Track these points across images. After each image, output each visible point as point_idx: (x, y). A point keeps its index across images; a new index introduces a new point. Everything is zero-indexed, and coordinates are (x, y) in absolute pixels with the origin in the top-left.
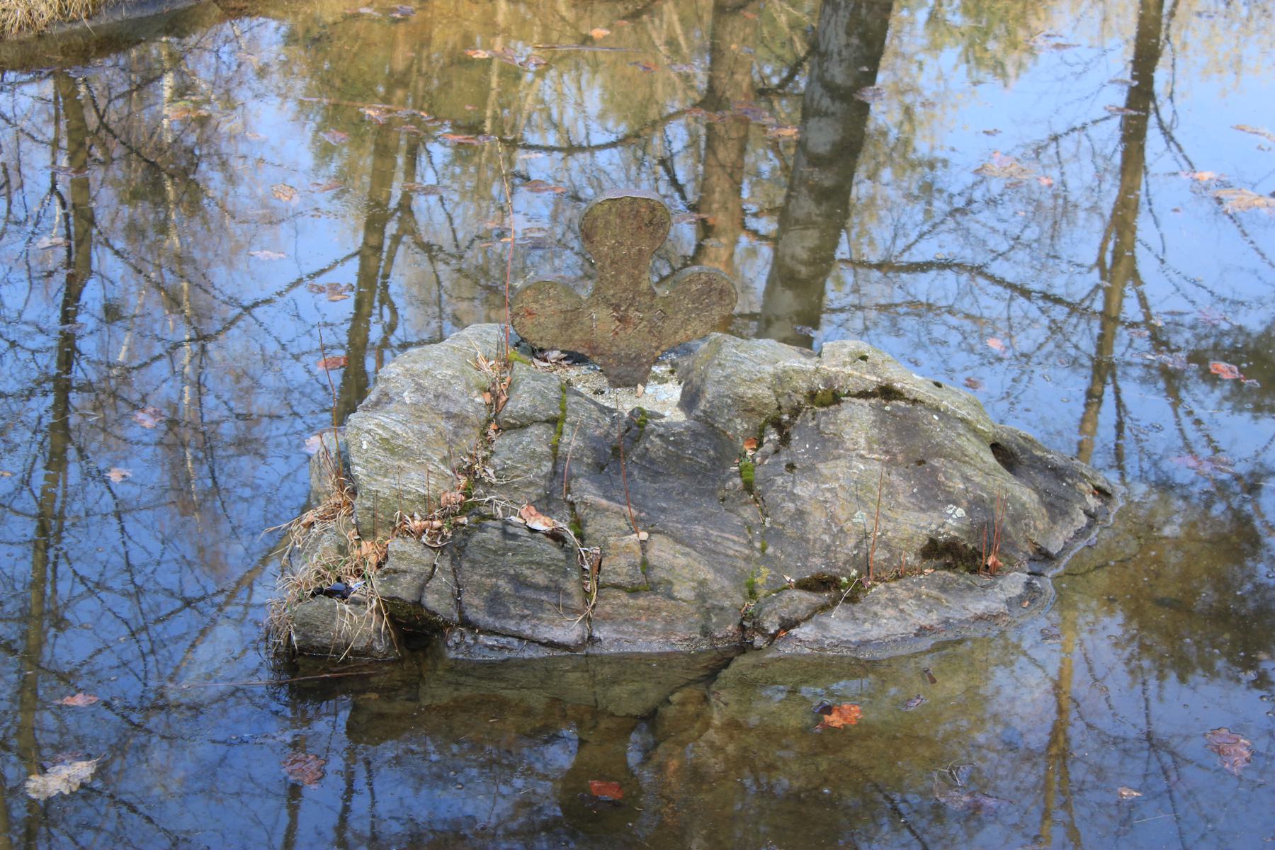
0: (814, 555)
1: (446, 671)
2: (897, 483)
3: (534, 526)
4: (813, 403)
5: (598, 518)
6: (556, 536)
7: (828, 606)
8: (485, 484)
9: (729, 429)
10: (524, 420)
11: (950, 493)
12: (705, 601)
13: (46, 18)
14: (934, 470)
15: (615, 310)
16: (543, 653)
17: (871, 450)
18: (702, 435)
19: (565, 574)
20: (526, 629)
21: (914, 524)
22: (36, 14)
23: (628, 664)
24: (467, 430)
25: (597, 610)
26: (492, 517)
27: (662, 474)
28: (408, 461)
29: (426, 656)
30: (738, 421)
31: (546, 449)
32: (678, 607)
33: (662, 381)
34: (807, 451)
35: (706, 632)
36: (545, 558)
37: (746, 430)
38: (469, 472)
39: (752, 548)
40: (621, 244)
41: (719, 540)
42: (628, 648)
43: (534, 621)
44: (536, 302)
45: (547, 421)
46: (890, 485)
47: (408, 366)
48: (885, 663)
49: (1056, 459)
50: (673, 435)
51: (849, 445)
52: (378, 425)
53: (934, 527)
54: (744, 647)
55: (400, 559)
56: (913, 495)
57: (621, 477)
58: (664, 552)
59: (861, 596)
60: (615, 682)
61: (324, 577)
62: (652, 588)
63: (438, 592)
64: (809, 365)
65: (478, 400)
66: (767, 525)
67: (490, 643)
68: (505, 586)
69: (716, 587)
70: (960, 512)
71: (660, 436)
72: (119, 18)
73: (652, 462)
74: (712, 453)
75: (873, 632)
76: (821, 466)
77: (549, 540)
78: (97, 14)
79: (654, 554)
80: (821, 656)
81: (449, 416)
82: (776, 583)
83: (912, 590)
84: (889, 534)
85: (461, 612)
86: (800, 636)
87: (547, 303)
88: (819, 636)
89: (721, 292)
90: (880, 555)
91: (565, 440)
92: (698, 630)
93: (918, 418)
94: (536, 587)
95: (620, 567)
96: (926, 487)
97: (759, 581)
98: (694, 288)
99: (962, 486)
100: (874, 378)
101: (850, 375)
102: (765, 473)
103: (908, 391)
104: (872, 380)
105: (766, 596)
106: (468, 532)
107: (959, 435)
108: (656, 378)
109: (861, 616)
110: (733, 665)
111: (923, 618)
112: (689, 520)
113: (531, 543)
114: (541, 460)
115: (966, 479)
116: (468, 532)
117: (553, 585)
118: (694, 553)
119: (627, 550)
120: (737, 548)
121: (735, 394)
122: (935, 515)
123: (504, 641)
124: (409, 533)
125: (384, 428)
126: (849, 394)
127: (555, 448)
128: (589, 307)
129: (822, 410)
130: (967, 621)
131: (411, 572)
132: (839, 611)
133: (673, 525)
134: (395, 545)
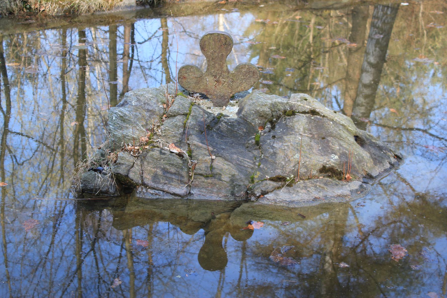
0: (278, 169)
1: (135, 201)
2: (313, 145)
3: (173, 151)
4: (285, 115)
5: (198, 150)
6: (180, 155)
7: (280, 187)
8: (157, 135)
9: (253, 122)
10: (175, 114)
11: (333, 150)
12: (233, 182)
13: (94, 9)
14: (328, 141)
15: (215, 78)
16: (171, 197)
17: (305, 133)
18: (242, 124)
19: (182, 169)
20: (166, 188)
21: (318, 160)
22: (91, 8)
23: (202, 204)
24: (155, 116)
25: (193, 183)
26: (158, 147)
27: (225, 136)
28: (130, 125)
29: (130, 196)
30: (257, 120)
31: (181, 124)
32: (223, 184)
33: (233, 105)
34: (281, 132)
35: (233, 194)
36: (175, 163)
37: (260, 123)
38: (152, 130)
39: (254, 163)
40: (215, 52)
41: (242, 161)
42: (202, 198)
43: (169, 185)
44: (186, 73)
45: (183, 114)
46: (311, 146)
47: (135, 92)
48: (299, 209)
49: (380, 143)
50: (230, 122)
51: (296, 130)
52: (119, 111)
53: (325, 161)
54: (247, 200)
55: (121, 159)
56: (319, 150)
57: (209, 136)
58: (219, 163)
59: (293, 184)
60: (196, 209)
61: (94, 164)
62: (213, 176)
63: (134, 172)
64: (285, 101)
65: (161, 106)
66: (262, 157)
67: (152, 192)
68: (159, 172)
69: (238, 177)
70: (336, 157)
71: (225, 122)
72: (118, 11)
73: (221, 132)
74: (245, 130)
75: (295, 197)
76: (285, 137)
77: (177, 156)
78: (112, 9)
79: (215, 164)
80: (275, 206)
81: (148, 111)
82: (262, 178)
83: (313, 184)
84: (307, 163)
85: (142, 180)
86: (268, 197)
87: (190, 74)
88: (275, 198)
89: (254, 72)
90: (302, 170)
91: (189, 121)
92: (230, 193)
93: (324, 122)
94: (171, 173)
95: (202, 167)
96: (325, 147)
97: (256, 177)
98: (243, 70)
99: (338, 148)
100: (309, 107)
101: (300, 105)
102: (264, 139)
103: (321, 112)
104: (308, 107)
105: (257, 182)
106: (148, 151)
107: (340, 130)
108: (231, 104)
109: (292, 192)
110: (241, 207)
111: (315, 194)
112: (232, 153)
113: (170, 156)
114: (179, 128)
115: (340, 145)
116: (148, 151)
117: (177, 173)
118: (231, 165)
119: (205, 162)
120: (249, 164)
121: (256, 109)
122: (326, 157)
123: (157, 192)
124: (126, 150)
125: (122, 112)
126: (299, 112)
127: (185, 124)
128: (206, 76)
129: (288, 117)
130: (334, 197)
131: (125, 164)
132: (284, 190)
133: (226, 154)
134: (121, 154)
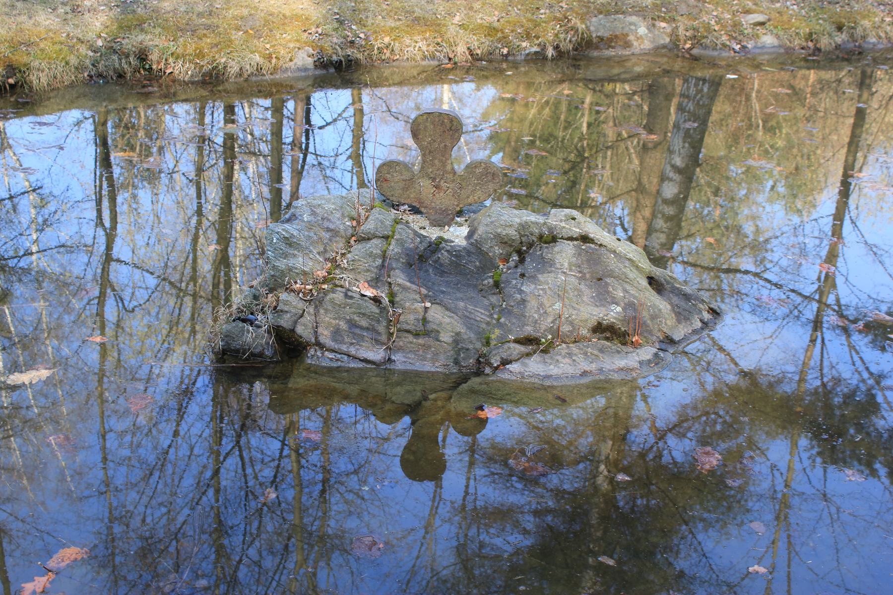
0: (527, 325)
6: (376, 300)
8: (341, 268)
14: (607, 284)
16: (361, 365)
19: (378, 321)
20: (353, 351)
21: (591, 312)
23: (410, 376)
26: (341, 286)
30: (497, 248)
32: (442, 346)
33: (460, 225)
34: (534, 267)
35: (456, 362)
36: (367, 311)
37: (501, 254)
38: (334, 261)
39: (491, 316)
42: (409, 367)
43: (358, 347)
46: (580, 290)
48: (559, 389)
49: (688, 289)
51: (558, 266)
53: (601, 315)
54: (479, 373)
56: (593, 297)
58: (436, 314)
59: (551, 350)
60: (398, 384)
61: (242, 311)
62: (427, 333)
63: (304, 325)
64: (541, 219)
68: (343, 325)
69: (466, 337)
70: (619, 309)
71: (448, 251)
73: (441, 265)
75: (554, 370)
76: (539, 276)
81: (328, 230)
85: (316, 338)
88: (522, 370)
90: (565, 328)
91: (391, 248)
94: (361, 328)
95: (409, 320)
96: (601, 294)
97: (493, 336)
98: (478, 171)
101: (564, 227)
104: (576, 231)
106: (326, 293)
108: (456, 223)
110: (469, 382)
111: (585, 365)
112: (457, 299)
113: (361, 302)
115: (625, 291)
116: (326, 293)
119: (415, 311)
122: (603, 309)
123: (339, 356)
124: (293, 291)
125: (287, 232)
126: (562, 238)
130: (614, 371)
132: (536, 357)
133: (447, 300)
134: (283, 296)
